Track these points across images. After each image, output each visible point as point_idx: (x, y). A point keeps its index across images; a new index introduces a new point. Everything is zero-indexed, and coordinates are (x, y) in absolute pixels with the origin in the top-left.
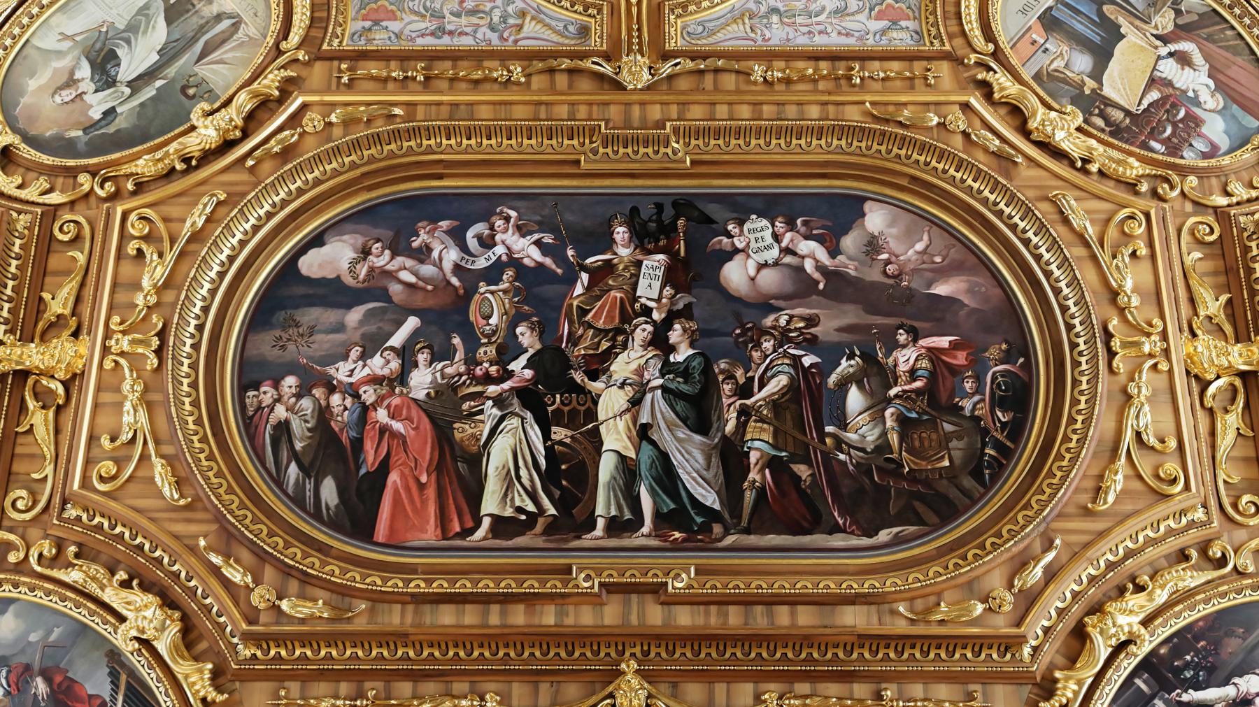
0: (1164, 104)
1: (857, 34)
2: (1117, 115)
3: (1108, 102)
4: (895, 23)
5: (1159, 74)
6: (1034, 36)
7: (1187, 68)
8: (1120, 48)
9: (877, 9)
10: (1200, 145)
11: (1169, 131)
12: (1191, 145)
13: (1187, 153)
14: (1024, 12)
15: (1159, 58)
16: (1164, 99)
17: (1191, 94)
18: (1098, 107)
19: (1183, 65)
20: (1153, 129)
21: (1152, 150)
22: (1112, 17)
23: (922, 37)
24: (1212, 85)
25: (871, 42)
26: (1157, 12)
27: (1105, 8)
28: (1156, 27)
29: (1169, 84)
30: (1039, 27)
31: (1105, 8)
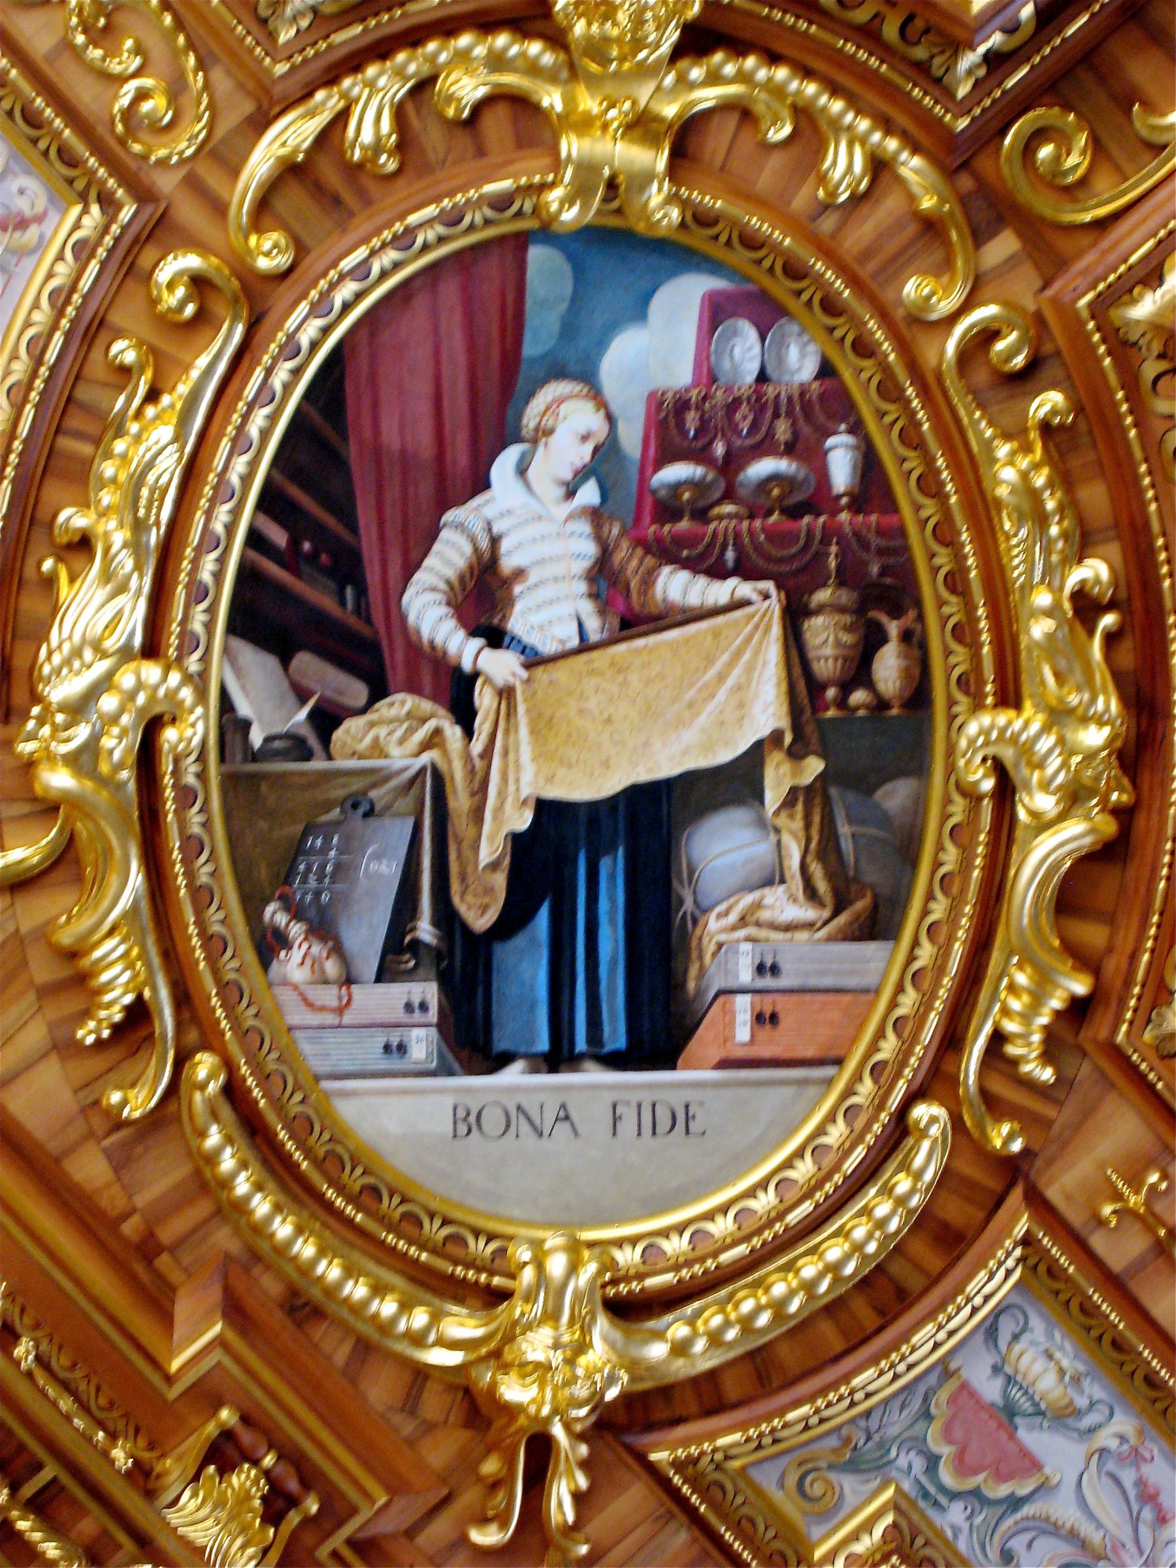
0: (680, 541)
1: (1128, 1477)
2: (826, 637)
3: (803, 686)
4: (1010, 1411)
5: (593, 626)
6: (743, 1033)
7: (508, 564)
8: (589, 784)
9: (1003, 1490)
10: (744, 351)
11: (762, 468)
12: (762, 377)
13: (800, 363)
14: (683, 1120)
15: (534, 660)
16: (668, 553)
17: (589, 494)
18: (842, 703)
19: (507, 583)
20: (794, 512)
21: (869, 465)
22: (500, 880)
23: (998, 1313)
24: (510, 456)
25: (1124, 1423)
26: (380, 777)
27: (481, 921)
28: (435, 740)
29: (603, 577)
30: (705, 1042)
31: (481, 921)
